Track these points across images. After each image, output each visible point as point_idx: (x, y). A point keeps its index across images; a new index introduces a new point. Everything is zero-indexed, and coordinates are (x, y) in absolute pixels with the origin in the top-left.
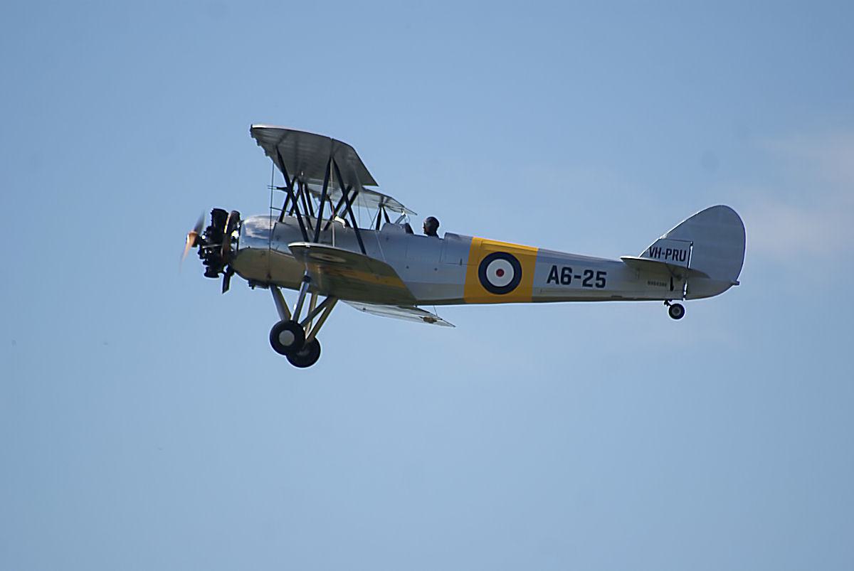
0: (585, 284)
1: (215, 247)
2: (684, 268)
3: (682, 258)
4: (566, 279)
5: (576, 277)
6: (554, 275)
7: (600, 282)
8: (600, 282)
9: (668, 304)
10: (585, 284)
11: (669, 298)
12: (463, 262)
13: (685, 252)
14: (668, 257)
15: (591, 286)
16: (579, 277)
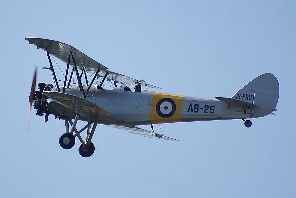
0: (205, 112)
1: (40, 100)
2: (251, 103)
3: (250, 99)
4: (196, 110)
5: (201, 109)
6: (191, 108)
7: (212, 111)
8: (212, 111)
9: (244, 121)
10: (205, 112)
11: (244, 117)
12: (149, 104)
13: (251, 95)
14: (244, 98)
15: (208, 112)
16: (201, 109)
